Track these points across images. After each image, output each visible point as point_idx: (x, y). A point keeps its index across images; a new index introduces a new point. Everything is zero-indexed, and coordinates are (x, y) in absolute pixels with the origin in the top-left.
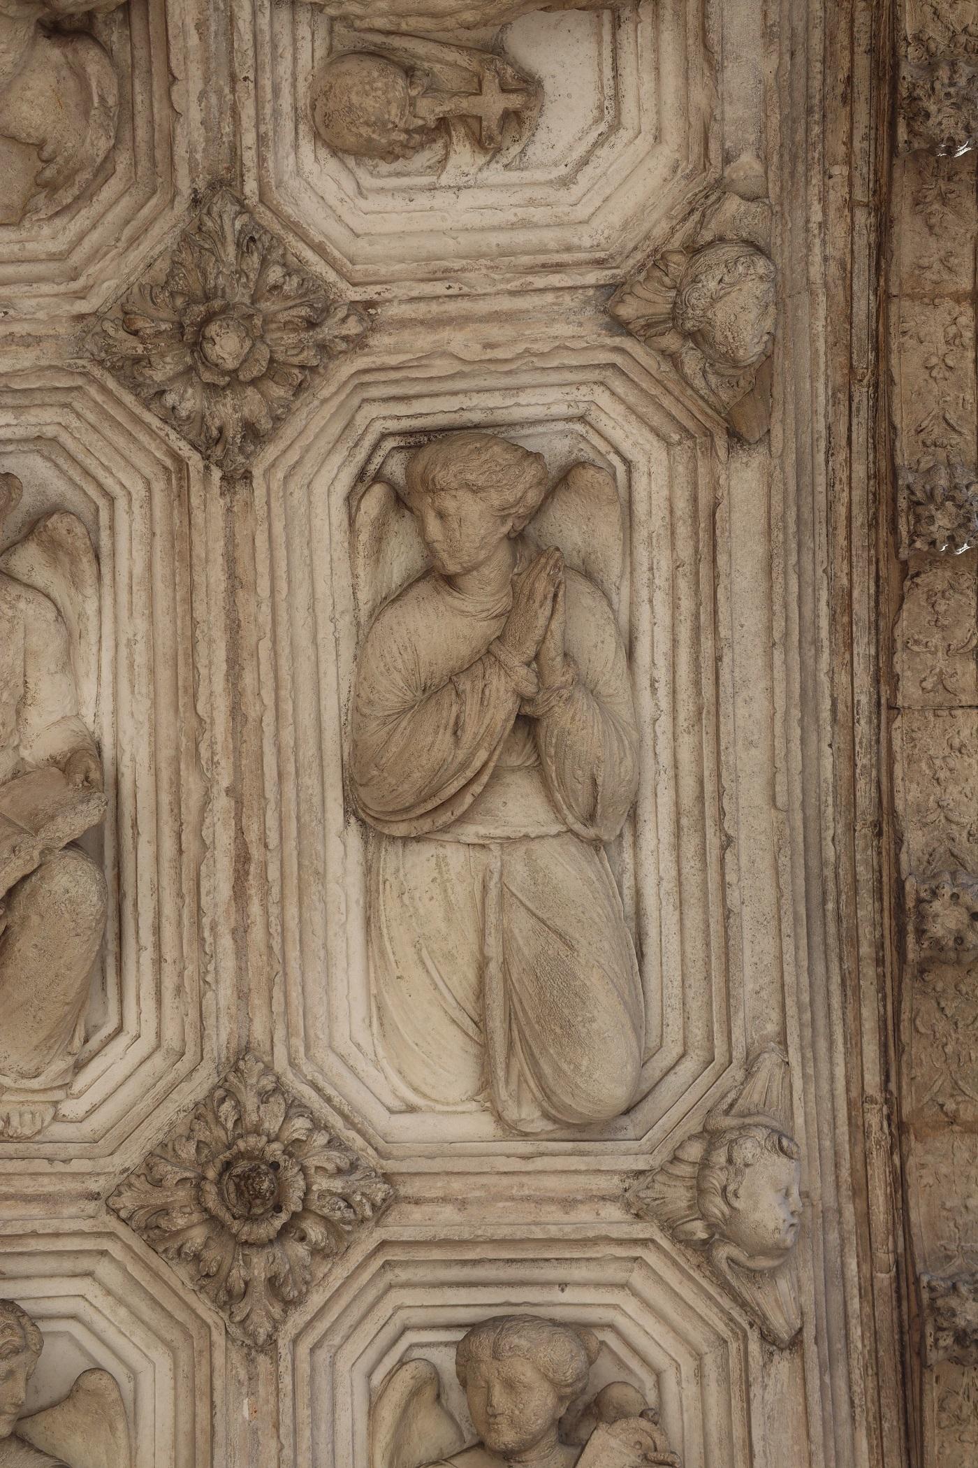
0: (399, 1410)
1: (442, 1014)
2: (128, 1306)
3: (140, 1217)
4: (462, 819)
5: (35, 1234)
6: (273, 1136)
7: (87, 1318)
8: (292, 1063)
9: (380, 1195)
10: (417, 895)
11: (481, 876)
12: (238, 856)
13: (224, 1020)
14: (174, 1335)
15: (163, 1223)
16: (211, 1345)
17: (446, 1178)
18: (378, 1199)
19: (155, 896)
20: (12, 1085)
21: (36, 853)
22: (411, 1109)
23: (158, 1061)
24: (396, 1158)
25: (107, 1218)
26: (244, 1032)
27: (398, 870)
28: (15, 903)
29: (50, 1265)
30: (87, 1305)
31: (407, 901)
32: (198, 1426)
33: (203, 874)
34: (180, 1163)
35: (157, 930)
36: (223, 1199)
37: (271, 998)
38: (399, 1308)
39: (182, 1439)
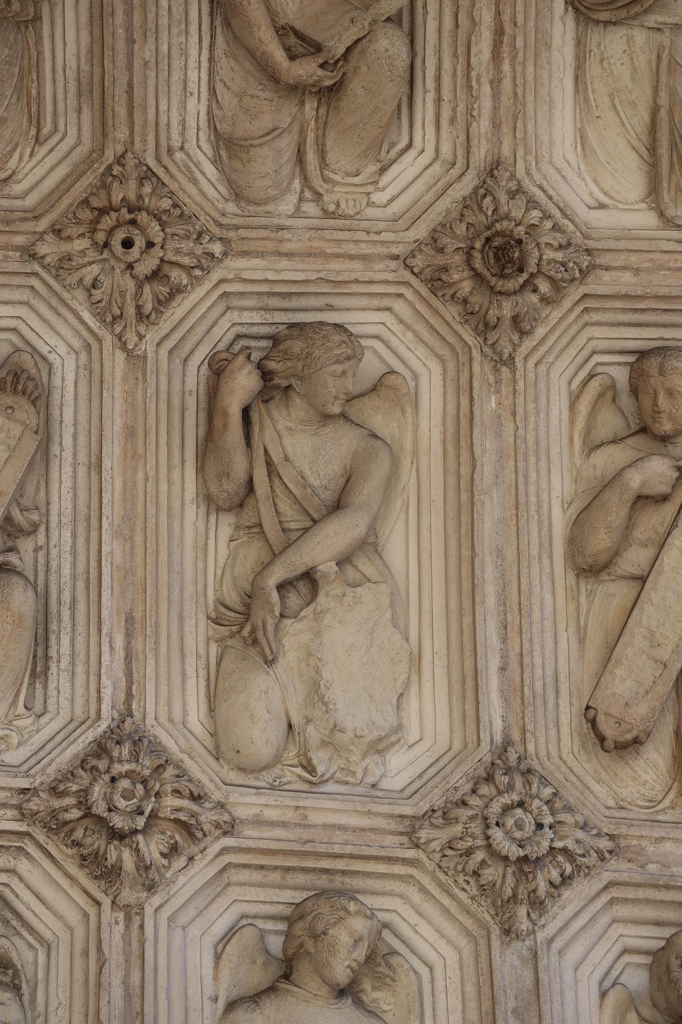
0: (590, 406)
1: (626, 143)
2: (413, 331)
3: (428, 273)
4: (646, 11)
5: (357, 281)
6: (518, 221)
7: (386, 338)
8: (528, 173)
9: (586, 264)
10: (613, 61)
11: (656, 50)
12: (496, 30)
13: (483, 142)
14: (445, 352)
15: (444, 277)
16: (471, 359)
17: (626, 254)
18: (584, 266)
19: (437, 56)
20: (341, 180)
21: (366, 24)
22: (602, 206)
23: (437, 168)
24: (595, 239)
25: (404, 272)
26: (496, 151)
27: (600, 44)
28: (350, 57)
29: (364, 302)
30: (386, 329)
31: (606, 65)
32: (461, 412)
33: (473, 42)
34: (455, 236)
35: (438, 79)
36: (485, 263)
37: (515, 128)
38: (590, 339)
39: (449, 420)
